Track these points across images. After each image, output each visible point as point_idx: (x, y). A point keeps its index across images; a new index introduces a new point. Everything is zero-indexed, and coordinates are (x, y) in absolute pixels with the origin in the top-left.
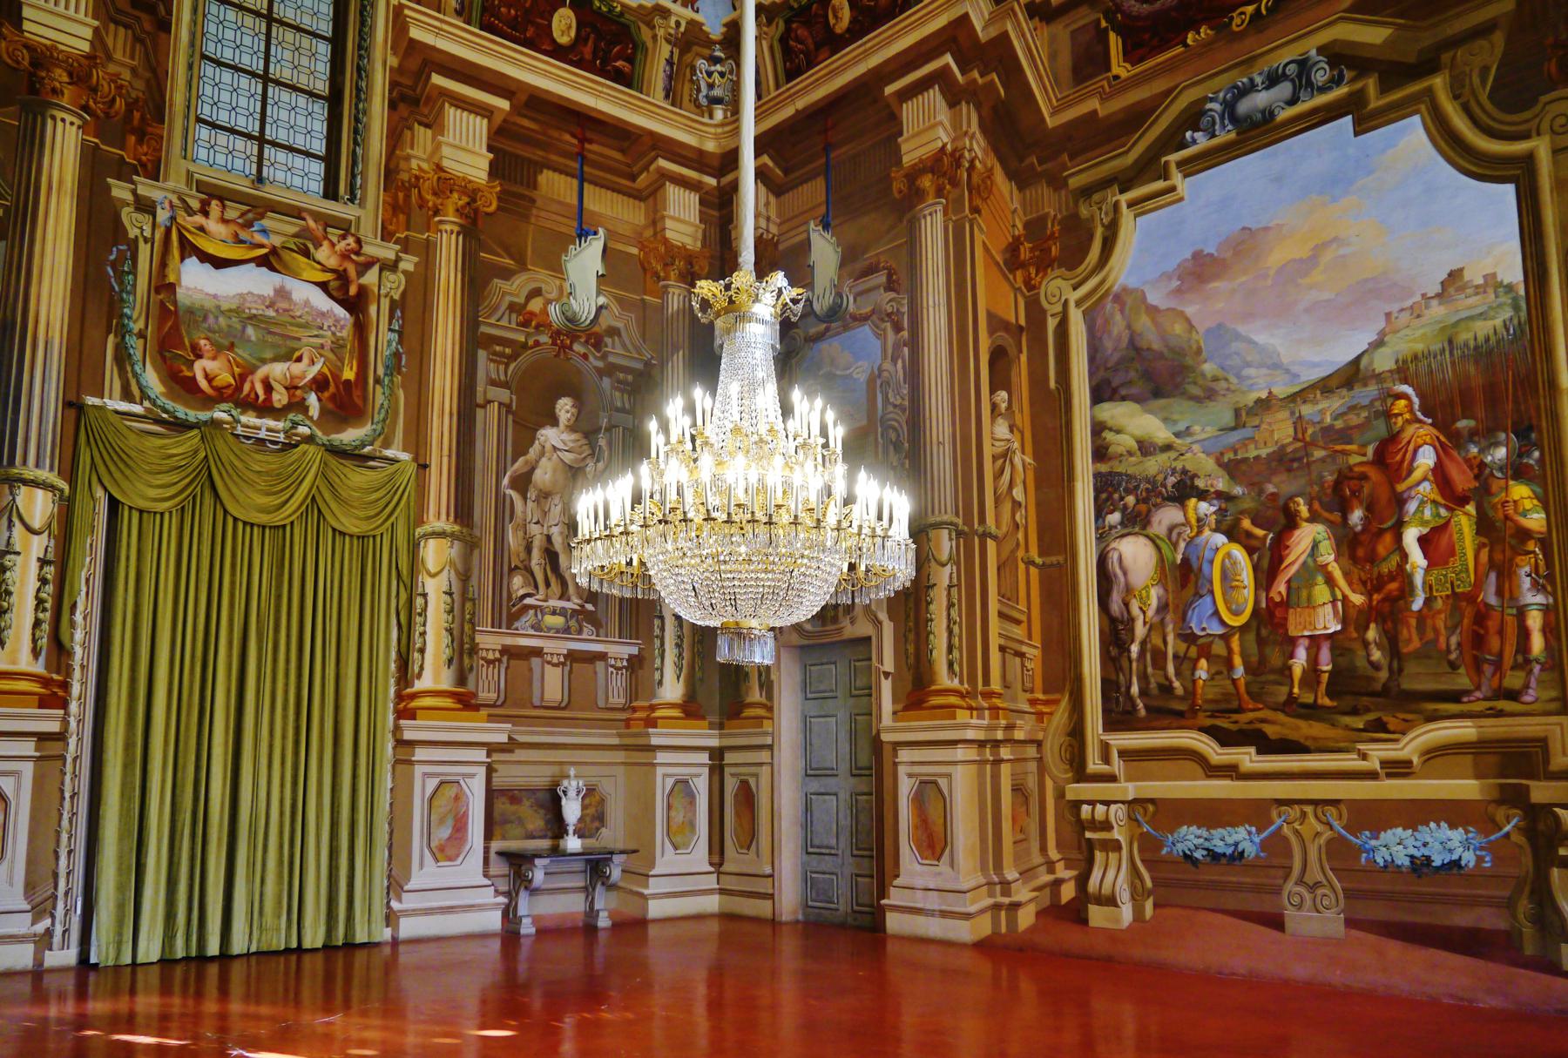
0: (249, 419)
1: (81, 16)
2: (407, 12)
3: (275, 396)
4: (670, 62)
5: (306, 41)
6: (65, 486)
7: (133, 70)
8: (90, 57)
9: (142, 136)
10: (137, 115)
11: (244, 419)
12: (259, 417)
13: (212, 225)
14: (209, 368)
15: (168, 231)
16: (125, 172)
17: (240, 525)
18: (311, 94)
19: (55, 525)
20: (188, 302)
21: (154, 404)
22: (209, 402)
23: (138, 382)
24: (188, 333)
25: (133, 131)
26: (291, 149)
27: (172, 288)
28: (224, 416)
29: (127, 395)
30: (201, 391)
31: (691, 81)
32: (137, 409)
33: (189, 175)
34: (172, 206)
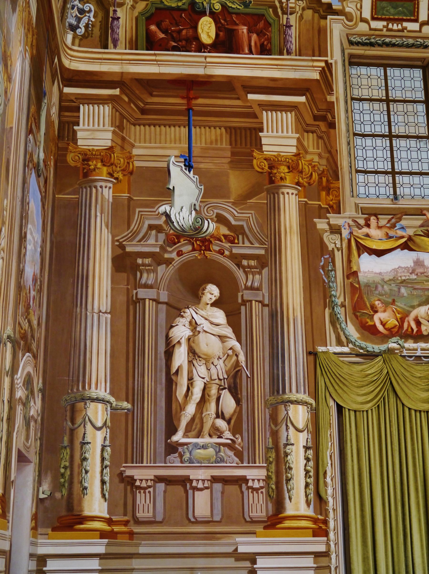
0: (410, 344)
1: (290, 134)
3: (423, 328)
5: (410, 107)
6: (313, 402)
7: (320, 155)
8: (297, 155)
9: (328, 190)
10: (324, 179)
11: (406, 345)
12: (415, 342)
13: (374, 232)
14: (383, 318)
15: (349, 241)
16: (322, 213)
17: (413, 412)
18: (418, 137)
19: (310, 426)
20: (365, 281)
21: (355, 345)
22: (385, 338)
23: (344, 333)
24: (368, 299)
25: (323, 189)
26: (411, 173)
27: (355, 274)
28: (395, 346)
29: (339, 343)
30: (379, 332)
32: (346, 350)
33: (357, 205)
34: (349, 226)
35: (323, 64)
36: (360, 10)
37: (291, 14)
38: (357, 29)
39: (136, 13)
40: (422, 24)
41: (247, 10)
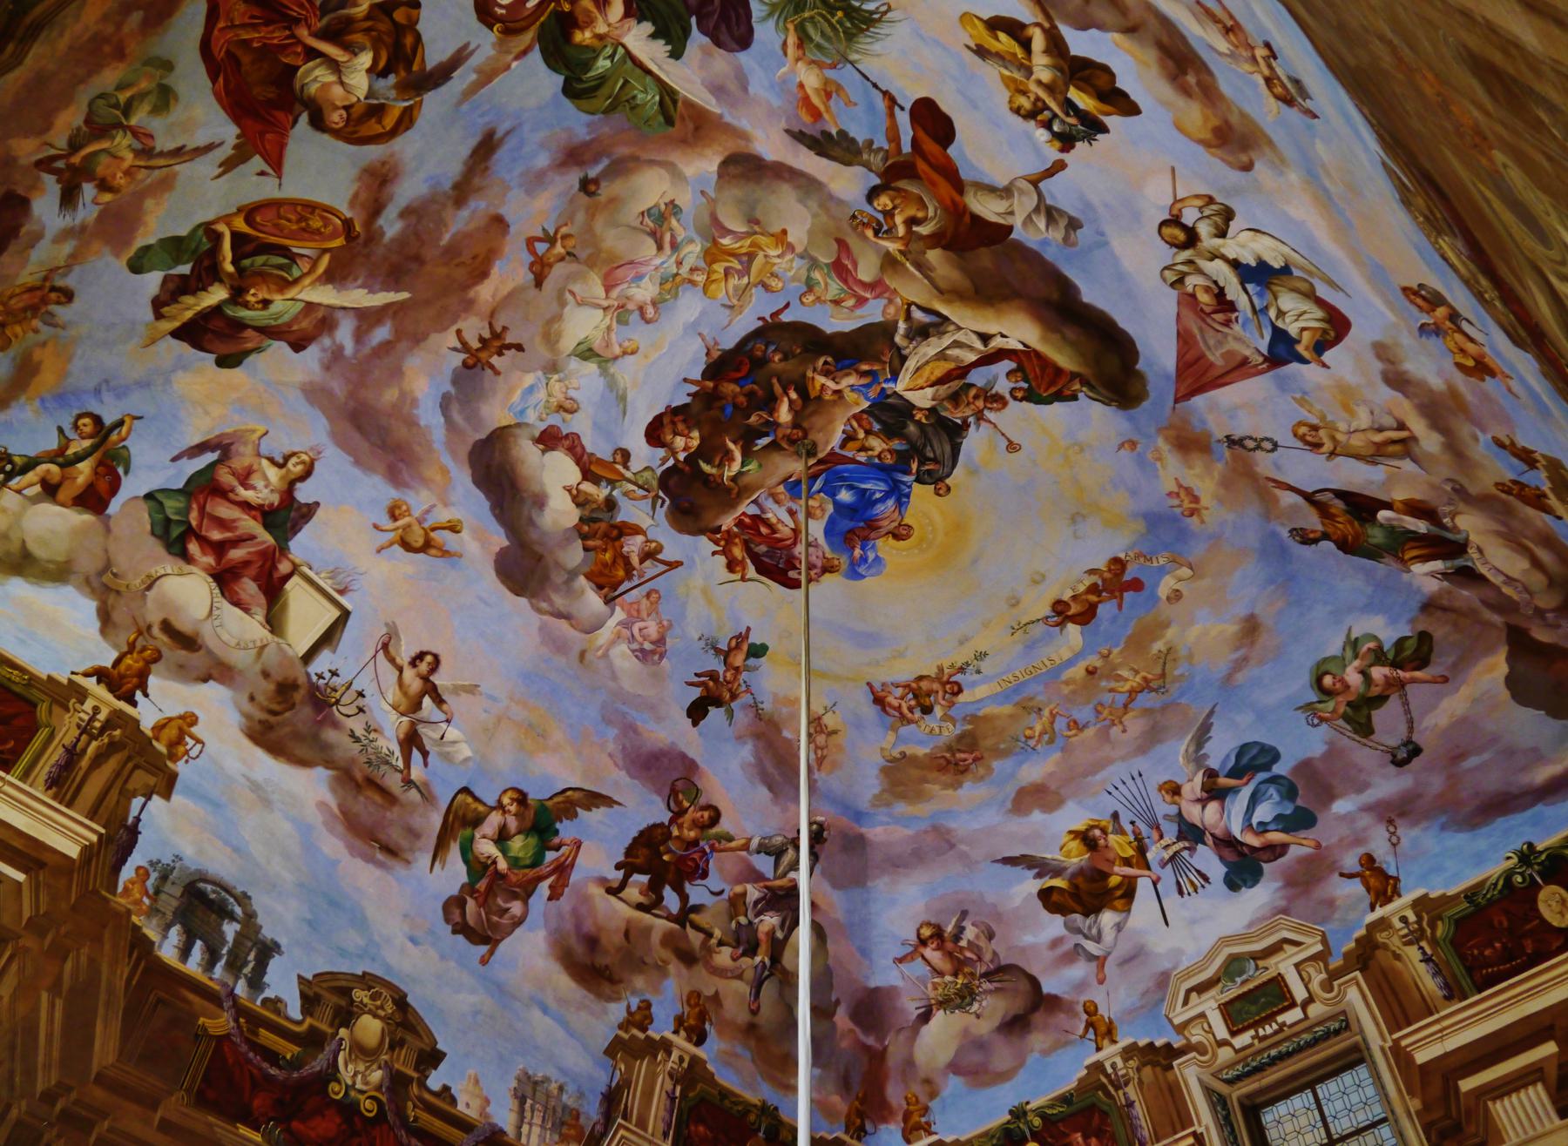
2: (1404, 1043)
35: (1191, 1140)
36: (1210, 1031)
37: (1126, 1084)
38: (1219, 1061)
40: (1305, 1005)
41: (1073, 1108)
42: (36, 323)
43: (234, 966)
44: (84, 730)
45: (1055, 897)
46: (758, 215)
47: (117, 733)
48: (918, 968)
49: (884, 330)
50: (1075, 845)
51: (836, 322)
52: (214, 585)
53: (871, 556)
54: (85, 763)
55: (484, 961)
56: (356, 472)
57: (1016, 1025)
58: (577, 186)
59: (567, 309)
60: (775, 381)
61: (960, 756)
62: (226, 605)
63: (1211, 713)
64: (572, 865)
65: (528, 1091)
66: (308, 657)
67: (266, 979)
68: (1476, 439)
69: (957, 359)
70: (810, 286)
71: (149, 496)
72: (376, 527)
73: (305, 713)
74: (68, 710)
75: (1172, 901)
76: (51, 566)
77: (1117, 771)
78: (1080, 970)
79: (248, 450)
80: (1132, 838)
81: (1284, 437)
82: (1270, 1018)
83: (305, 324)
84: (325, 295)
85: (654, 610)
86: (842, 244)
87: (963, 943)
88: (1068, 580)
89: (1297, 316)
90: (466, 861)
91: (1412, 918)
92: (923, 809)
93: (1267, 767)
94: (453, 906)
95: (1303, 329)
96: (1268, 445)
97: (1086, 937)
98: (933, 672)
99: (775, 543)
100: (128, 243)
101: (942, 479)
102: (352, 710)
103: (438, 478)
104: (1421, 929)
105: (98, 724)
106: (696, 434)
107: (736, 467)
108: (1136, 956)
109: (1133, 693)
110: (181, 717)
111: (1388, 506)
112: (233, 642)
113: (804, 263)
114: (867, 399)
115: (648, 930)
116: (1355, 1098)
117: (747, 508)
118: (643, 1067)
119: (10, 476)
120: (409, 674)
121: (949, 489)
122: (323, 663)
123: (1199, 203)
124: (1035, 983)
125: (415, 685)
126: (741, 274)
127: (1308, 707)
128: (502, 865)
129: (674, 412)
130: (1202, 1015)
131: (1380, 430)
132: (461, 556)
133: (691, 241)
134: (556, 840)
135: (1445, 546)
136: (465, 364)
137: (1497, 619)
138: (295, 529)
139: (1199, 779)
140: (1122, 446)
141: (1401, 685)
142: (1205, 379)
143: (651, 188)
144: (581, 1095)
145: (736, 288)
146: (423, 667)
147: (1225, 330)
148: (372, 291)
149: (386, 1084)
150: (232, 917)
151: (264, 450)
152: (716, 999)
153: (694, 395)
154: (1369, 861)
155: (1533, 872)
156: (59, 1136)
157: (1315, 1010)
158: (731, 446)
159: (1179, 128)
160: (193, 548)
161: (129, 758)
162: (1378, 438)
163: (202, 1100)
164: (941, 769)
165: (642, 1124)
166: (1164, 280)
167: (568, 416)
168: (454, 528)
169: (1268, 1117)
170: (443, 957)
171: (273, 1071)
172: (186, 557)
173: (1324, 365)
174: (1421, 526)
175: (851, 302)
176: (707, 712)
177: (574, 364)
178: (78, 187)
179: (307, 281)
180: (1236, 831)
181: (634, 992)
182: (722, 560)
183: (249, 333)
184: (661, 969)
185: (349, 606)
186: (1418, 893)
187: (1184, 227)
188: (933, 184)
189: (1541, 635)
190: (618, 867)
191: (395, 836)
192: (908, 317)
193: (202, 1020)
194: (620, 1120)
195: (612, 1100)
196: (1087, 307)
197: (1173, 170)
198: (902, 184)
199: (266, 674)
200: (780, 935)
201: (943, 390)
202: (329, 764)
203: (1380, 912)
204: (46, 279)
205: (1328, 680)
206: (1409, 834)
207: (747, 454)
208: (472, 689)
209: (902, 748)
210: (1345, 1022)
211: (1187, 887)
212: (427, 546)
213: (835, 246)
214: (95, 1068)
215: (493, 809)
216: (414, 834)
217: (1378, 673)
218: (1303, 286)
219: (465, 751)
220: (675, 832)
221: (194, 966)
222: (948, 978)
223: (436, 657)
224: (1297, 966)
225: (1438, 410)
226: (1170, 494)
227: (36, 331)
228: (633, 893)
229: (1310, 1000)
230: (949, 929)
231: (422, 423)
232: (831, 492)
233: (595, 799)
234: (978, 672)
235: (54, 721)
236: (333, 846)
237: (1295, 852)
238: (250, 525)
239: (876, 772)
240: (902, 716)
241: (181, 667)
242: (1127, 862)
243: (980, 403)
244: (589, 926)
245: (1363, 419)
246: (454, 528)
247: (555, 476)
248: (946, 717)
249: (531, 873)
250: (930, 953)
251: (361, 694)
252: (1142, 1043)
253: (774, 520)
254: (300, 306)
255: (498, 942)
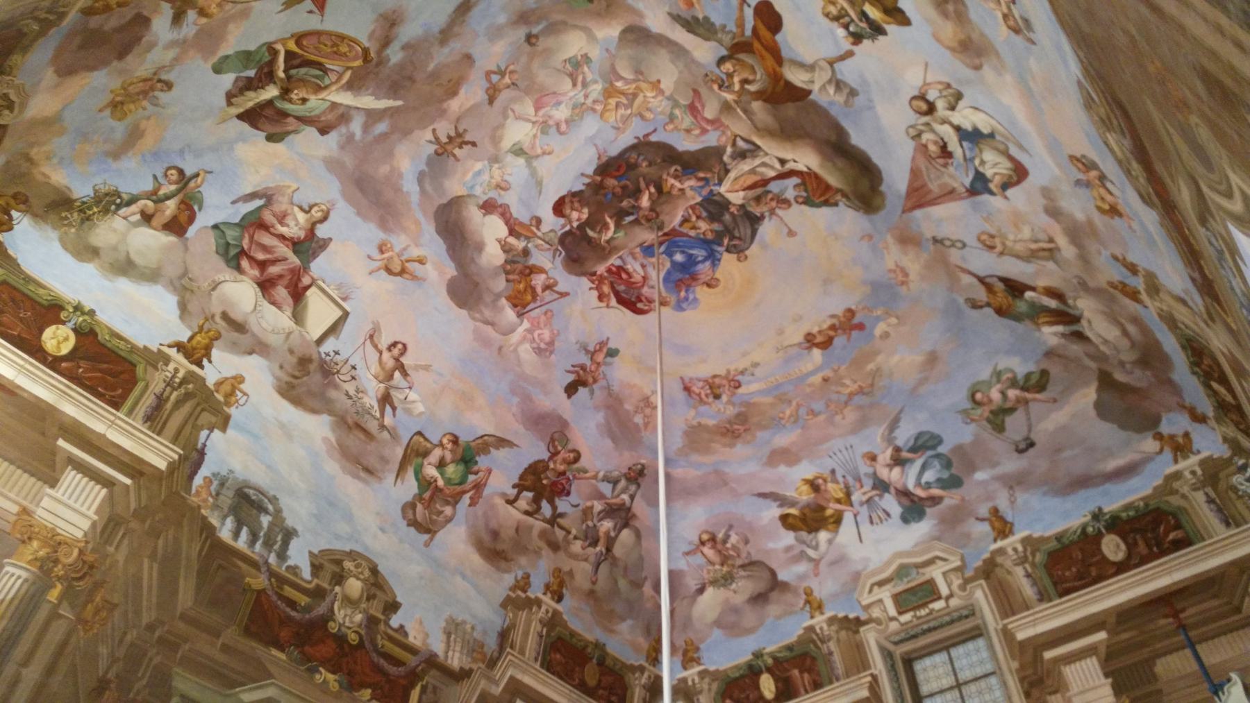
2: (1010, 626)
4: (1210, 501)
5: (982, 684)
31: (1240, 497)
35: (869, 679)
36: (885, 611)
39: (713, 694)
42: (145, 103)
43: (268, 544)
44: (169, 384)
45: (790, 520)
46: (643, 69)
47: (191, 386)
48: (698, 559)
49: (718, 152)
50: (805, 488)
51: (686, 144)
52: (258, 289)
53: (691, 297)
54: (169, 406)
55: (427, 545)
56: (359, 220)
57: (759, 599)
58: (523, 39)
59: (509, 121)
60: (641, 179)
61: (736, 427)
62: (265, 303)
63: (901, 411)
64: (485, 485)
65: (453, 629)
66: (320, 341)
67: (289, 553)
68: (1100, 254)
69: (762, 174)
70: (672, 118)
71: (216, 227)
72: (369, 257)
73: (316, 378)
74: (157, 369)
75: (866, 528)
76: (147, 271)
77: (837, 444)
78: (802, 568)
79: (285, 199)
80: (842, 486)
81: (971, 240)
82: (924, 605)
83: (330, 117)
84: (345, 98)
85: (548, 323)
86: (696, 92)
87: (729, 545)
88: (817, 322)
89: (993, 164)
90: (417, 479)
91: (1020, 548)
92: (707, 459)
93: (934, 447)
94: (409, 507)
95: (996, 174)
96: (959, 245)
97: (808, 546)
98: (723, 372)
99: (630, 285)
100: (213, 53)
101: (742, 251)
102: (347, 378)
103: (413, 227)
104: (1026, 557)
105: (177, 380)
106: (586, 210)
107: (610, 234)
108: (840, 560)
109: (851, 395)
110: (234, 378)
111: (1033, 289)
112: (270, 329)
113: (670, 103)
114: (700, 195)
115: (531, 528)
116: (975, 658)
117: (614, 261)
118: (523, 615)
119: (119, 207)
120: (386, 355)
121: (746, 257)
122: (329, 346)
123: (940, 87)
124: (773, 574)
125: (389, 362)
126: (626, 107)
127: (965, 412)
128: (441, 483)
129: (574, 195)
130: (881, 601)
131: (1036, 241)
132: (424, 280)
133: (596, 82)
134: (475, 468)
135: (1066, 317)
136: (436, 153)
137: (1093, 365)
138: (315, 255)
139: (889, 452)
140: (862, 238)
141: (1026, 402)
142: (923, 200)
143: (573, 44)
144: (485, 633)
145: (622, 116)
146: (396, 351)
147: (943, 169)
148: (378, 98)
149: (365, 623)
150: (266, 512)
151: (295, 200)
152: (571, 573)
153: (588, 185)
154: (995, 511)
155: (1101, 526)
156: (158, 653)
157: (954, 602)
158: (608, 220)
159: (938, 40)
160: (245, 263)
161: (198, 404)
162: (1034, 246)
163: (247, 632)
164: (723, 435)
165: (522, 652)
166: (908, 133)
167: (502, 193)
168: (421, 261)
169: (918, 666)
170: (401, 541)
171: (293, 614)
172: (239, 268)
173: (1006, 198)
174: (1053, 304)
175: (697, 132)
176: (577, 390)
177: (510, 158)
178: (184, 12)
179: (334, 88)
180: (911, 485)
181: (520, 567)
182: (595, 293)
183: (290, 120)
184: (537, 553)
185: (348, 309)
186: (1025, 533)
187: (927, 102)
188: (762, 57)
189: (1119, 376)
190: (514, 486)
191: (372, 462)
192: (734, 144)
193: (247, 579)
194: (508, 650)
195: (504, 635)
196: (853, 147)
197: (926, 65)
198: (742, 56)
199: (291, 352)
200: (613, 534)
201: (751, 193)
202: (330, 412)
203: (1000, 544)
204: (155, 74)
205: (979, 396)
206: (1021, 497)
207: (618, 226)
208: (427, 368)
209: (699, 420)
210: (971, 612)
211: (875, 519)
212: (403, 272)
213: (691, 93)
214: (179, 610)
215: (436, 446)
216: (384, 460)
217: (1013, 393)
218: (1002, 147)
219: (420, 408)
220: (552, 465)
221: (242, 544)
222: (717, 567)
223: (405, 346)
224: (944, 574)
225: (1076, 233)
226: (890, 271)
227: (144, 109)
228: (523, 504)
229: (951, 596)
230: (720, 536)
231: (405, 189)
232: (670, 254)
233: (502, 442)
234: (753, 375)
235: (148, 377)
236: (332, 467)
237: (947, 502)
238: (284, 250)
239: (680, 433)
240: (701, 399)
241: (234, 343)
242: (838, 501)
243: (774, 204)
244: (494, 524)
245: (1026, 233)
246: (421, 261)
247: (492, 231)
248: (729, 402)
249: (459, 489)
250: (707, 550)
251: (354, 368)
252: (841, 615)
253: (631, 270)
254: (328, 104)
255: (435, 532)
